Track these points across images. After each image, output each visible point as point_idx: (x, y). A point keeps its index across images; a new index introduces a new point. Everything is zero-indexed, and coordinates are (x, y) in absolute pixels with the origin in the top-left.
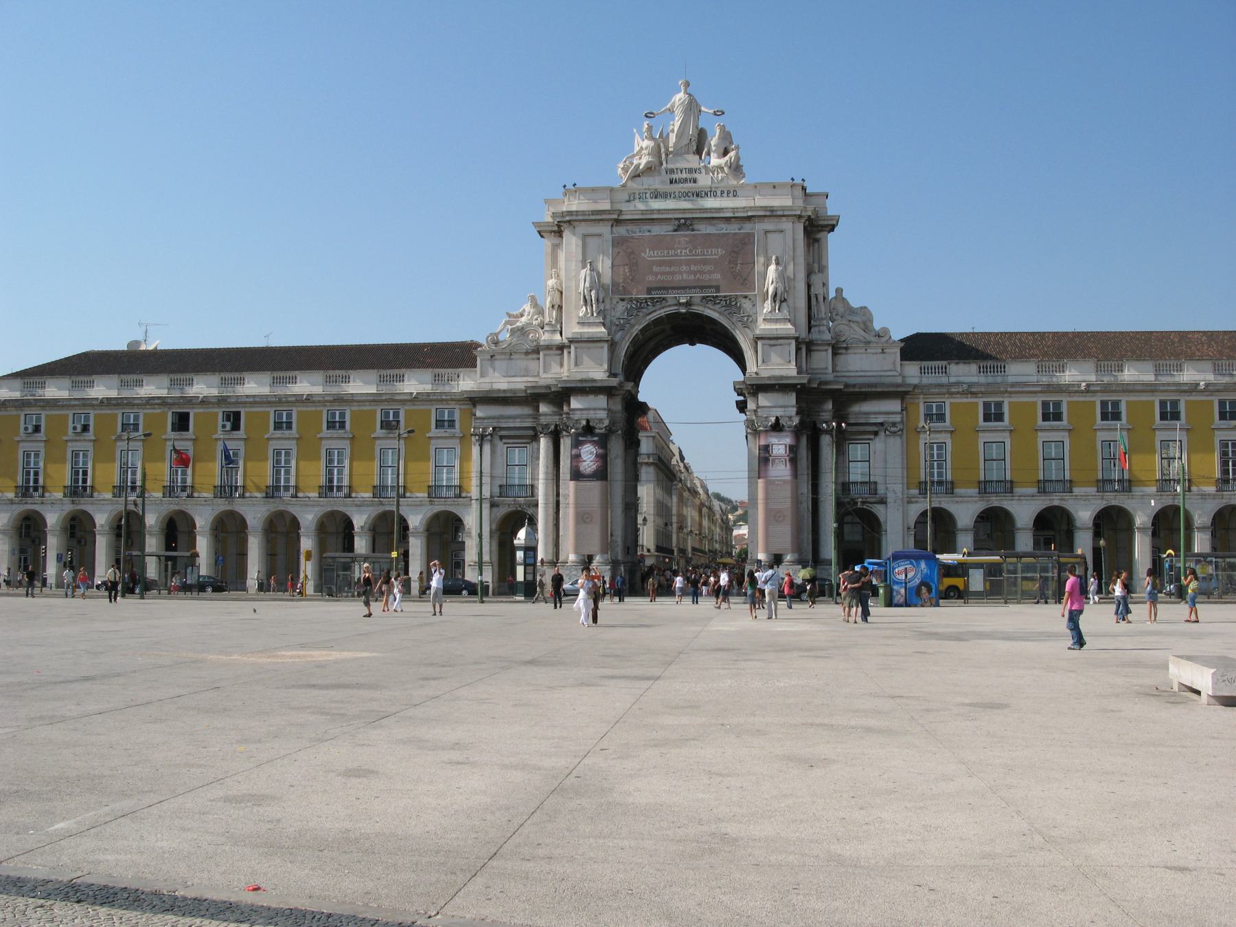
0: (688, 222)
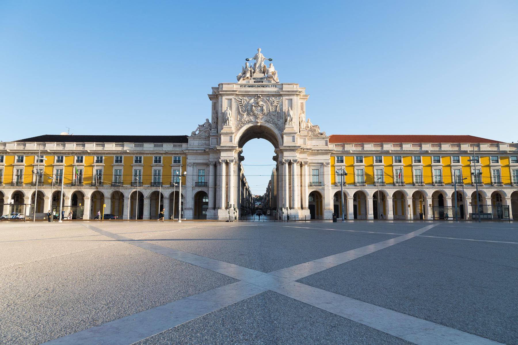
0: (261, 96)
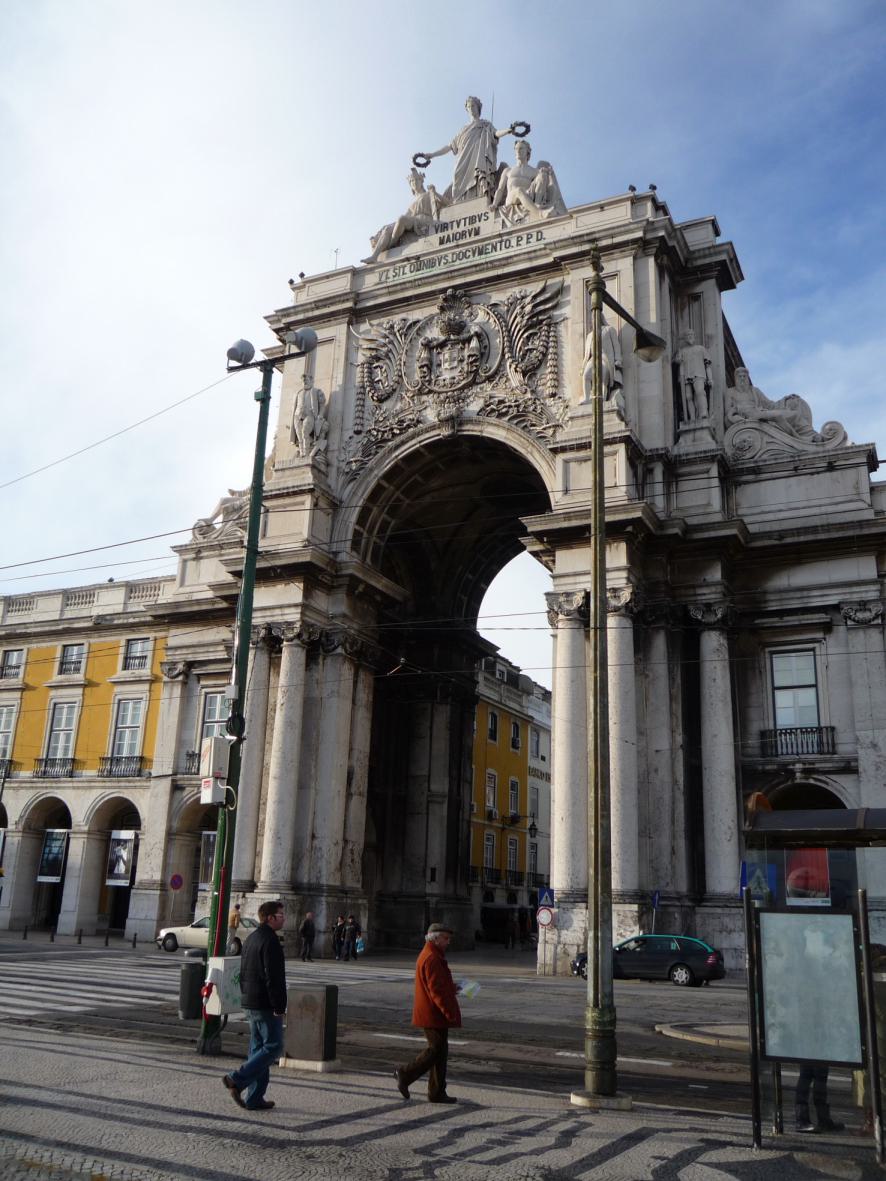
0: (459, 292)
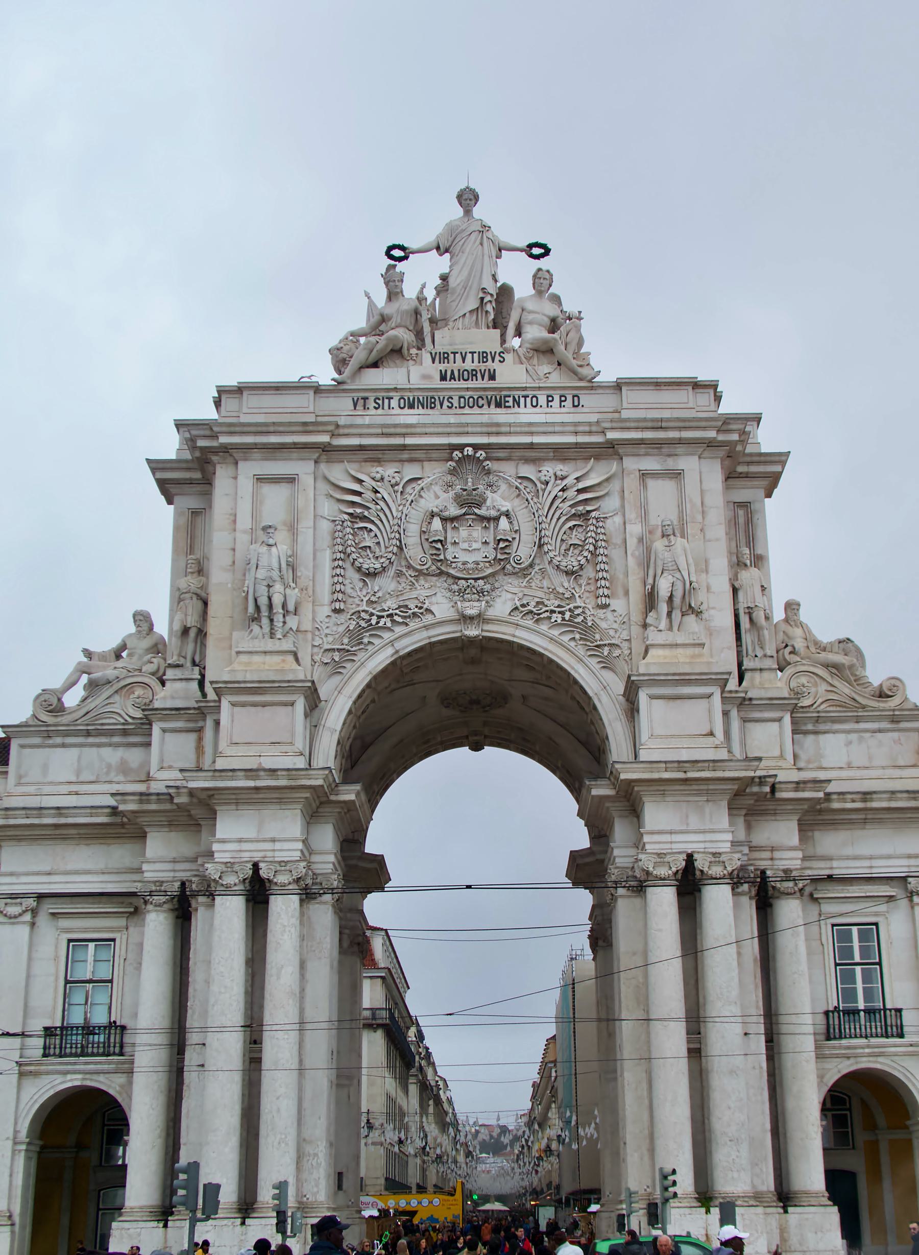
0: (481, 454)
